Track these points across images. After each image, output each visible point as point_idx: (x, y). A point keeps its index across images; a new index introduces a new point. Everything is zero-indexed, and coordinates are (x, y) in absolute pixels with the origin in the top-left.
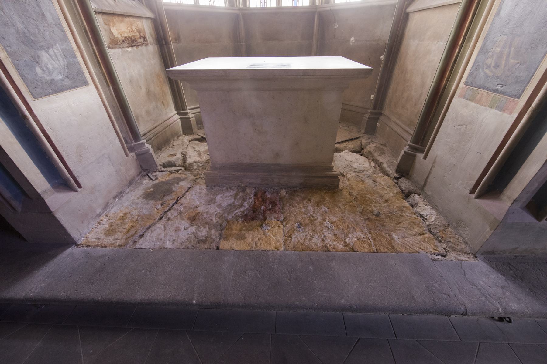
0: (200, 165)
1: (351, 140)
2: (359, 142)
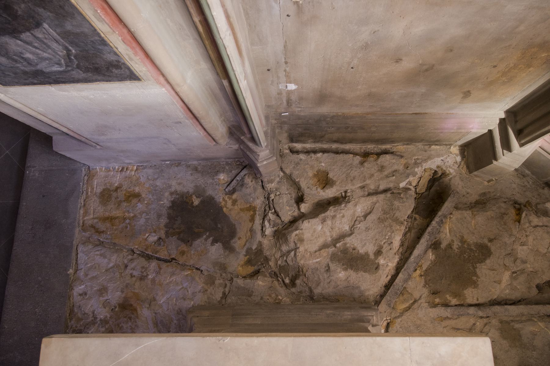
0: (289, 259)
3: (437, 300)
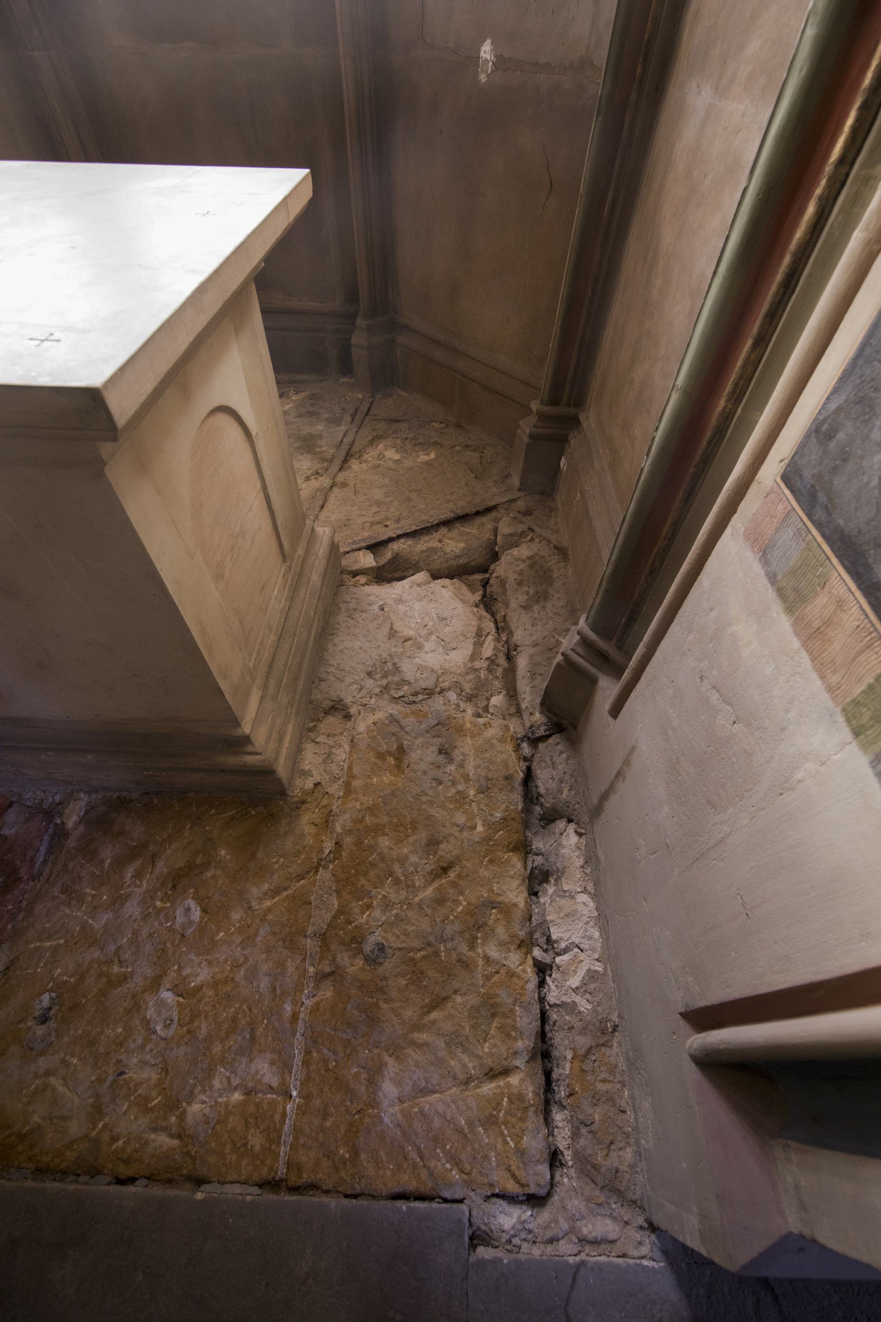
1: (463, 518)
2: (490, 526)
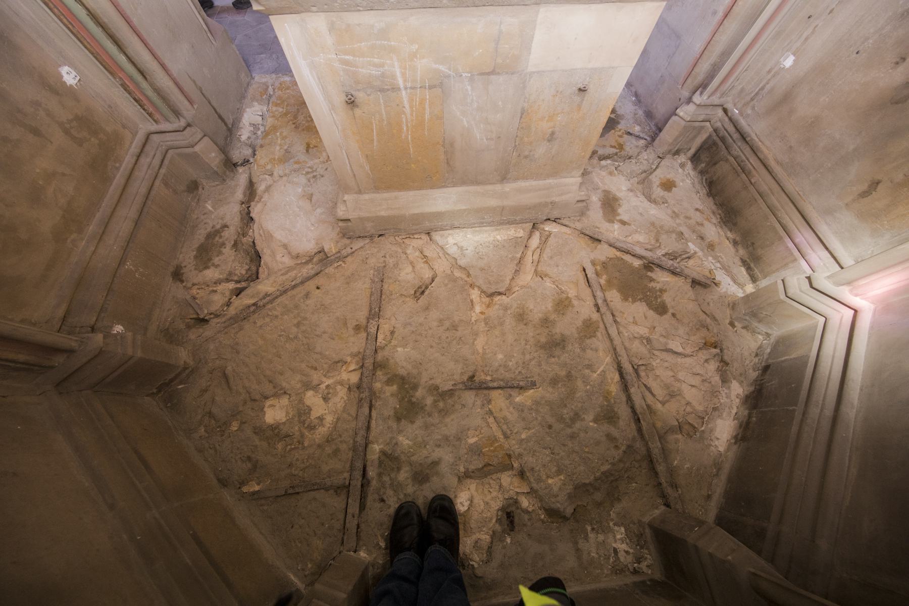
3: (598, 268)
